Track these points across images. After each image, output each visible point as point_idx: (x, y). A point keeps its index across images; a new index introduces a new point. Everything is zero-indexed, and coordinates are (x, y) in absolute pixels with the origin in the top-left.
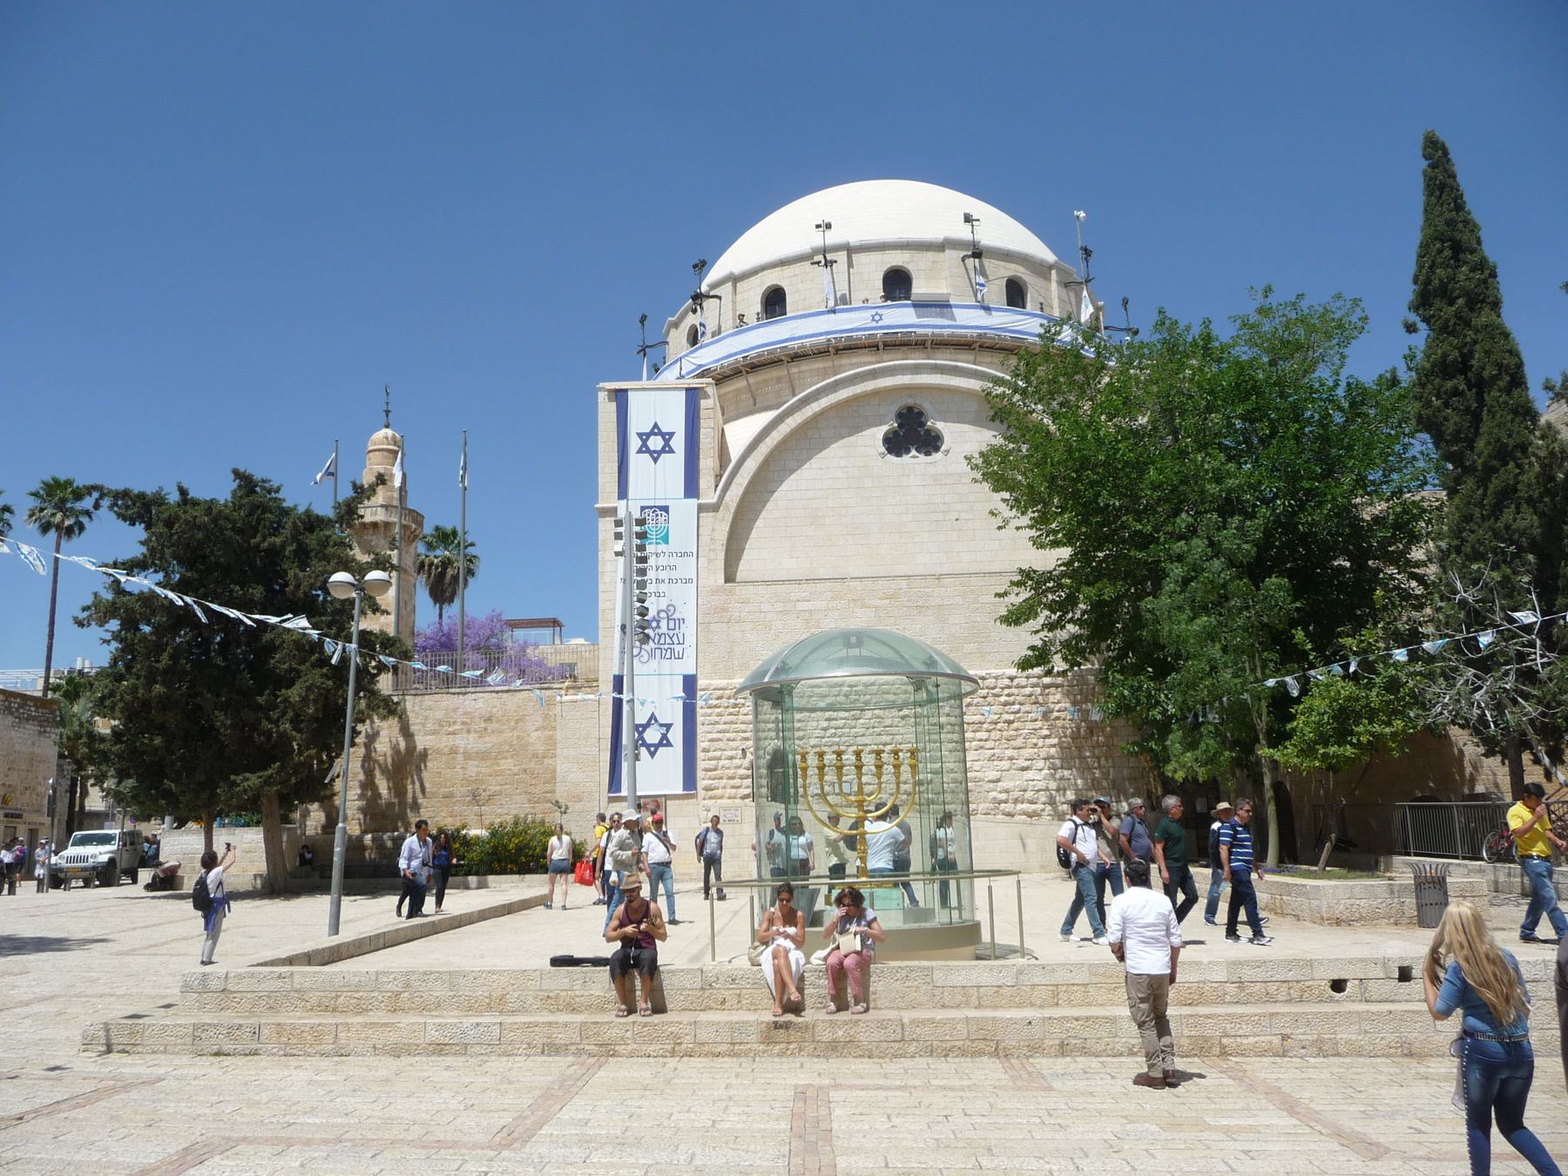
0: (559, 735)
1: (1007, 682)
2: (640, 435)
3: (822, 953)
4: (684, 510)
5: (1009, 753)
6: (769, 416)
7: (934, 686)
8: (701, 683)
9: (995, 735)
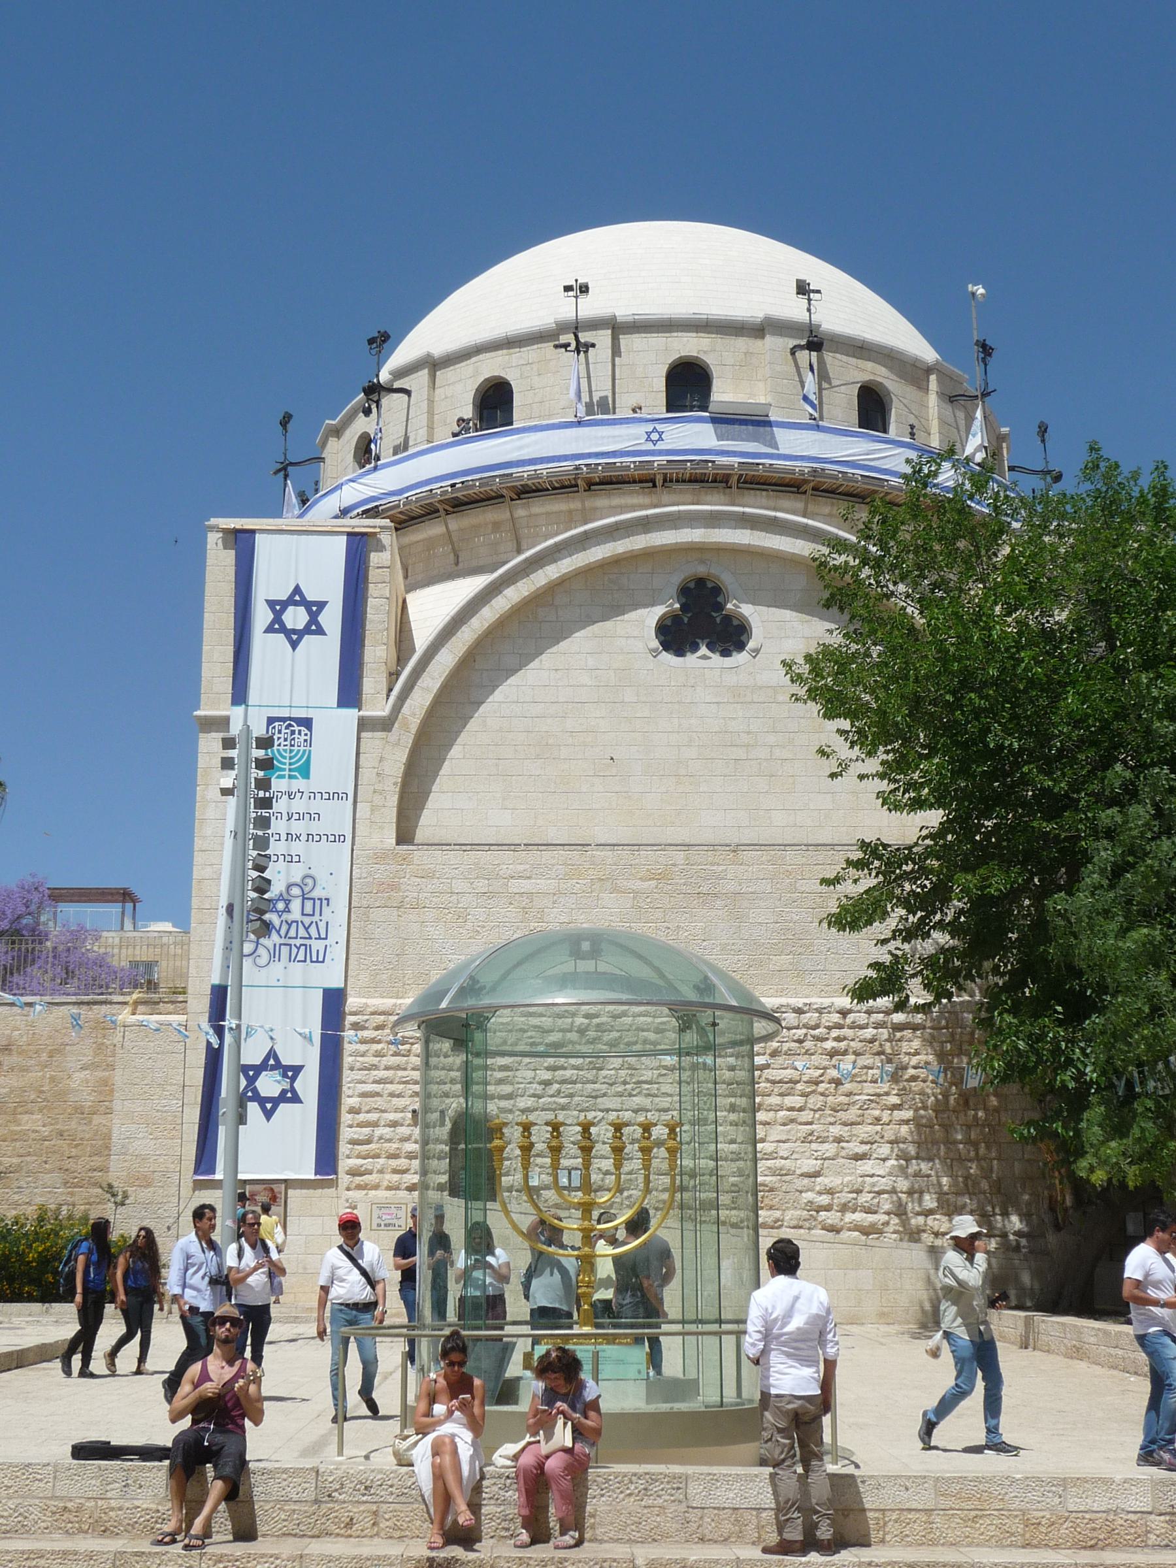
0: (118, 1077)
1: (836, 1018)
2: (271, 604)
3: (511, 1448)
4: (335, 727)
5: (836, 1130)
6: (479, 582)
7: (711, 1024)
8: (353, 1002)
9: (815, 1101)
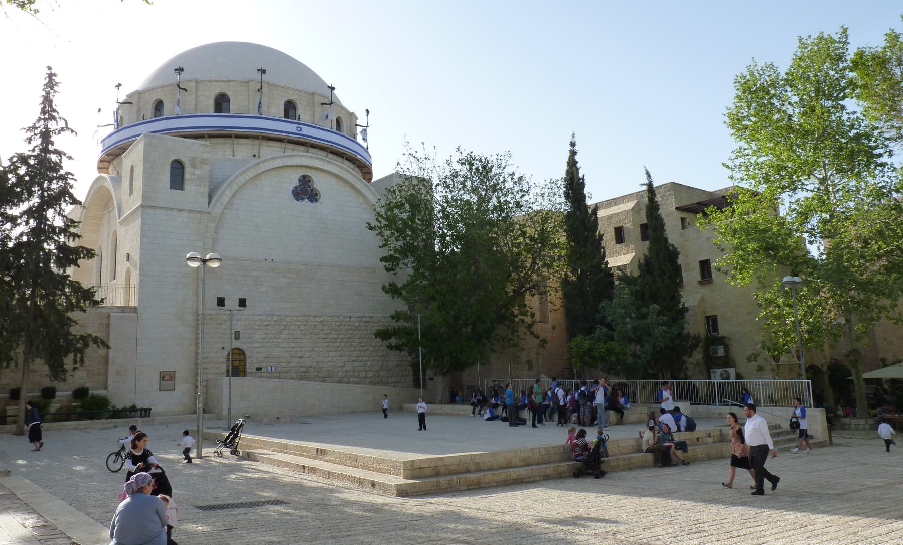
1: (348, 319)
5: (347, 353)
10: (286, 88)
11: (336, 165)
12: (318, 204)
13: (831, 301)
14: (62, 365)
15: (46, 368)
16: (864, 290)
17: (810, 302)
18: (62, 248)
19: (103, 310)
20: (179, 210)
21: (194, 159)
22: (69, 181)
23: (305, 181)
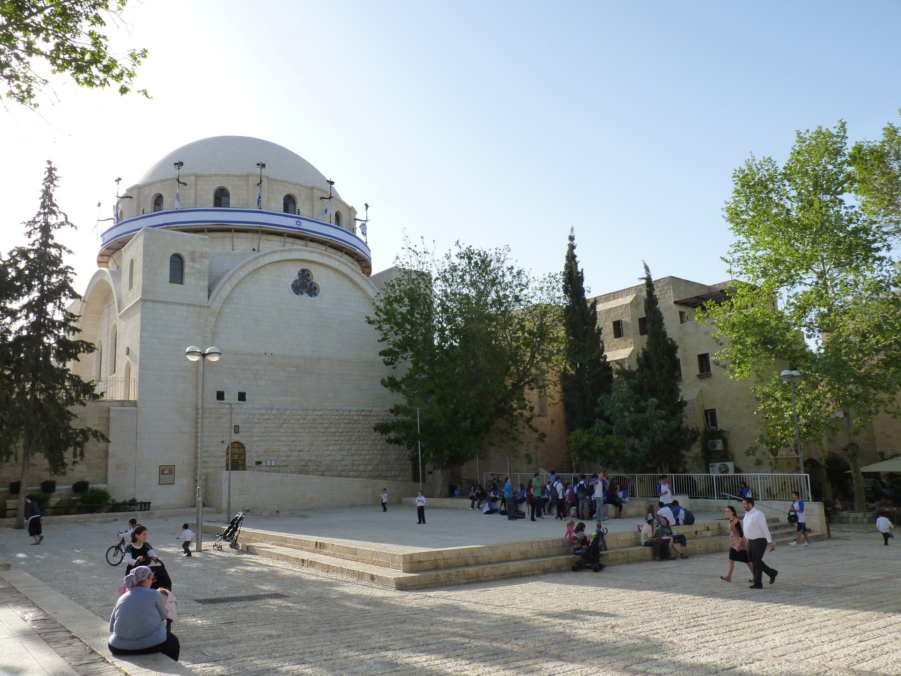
1: (347, 413)
5: (347, 447)
9: (342, 438)
10: (285, 182)
11: (335, 259)
12: (317, 298)
13: (829, 395)
14: (61, 459)
15: (46, 461)
16: (862, 384)
17: (808, 396)
18: (62, 342)
19: (103, 404)
20: (178, 304)
21: (193, 253)
22: (69, 275)
23: (304, 275)
